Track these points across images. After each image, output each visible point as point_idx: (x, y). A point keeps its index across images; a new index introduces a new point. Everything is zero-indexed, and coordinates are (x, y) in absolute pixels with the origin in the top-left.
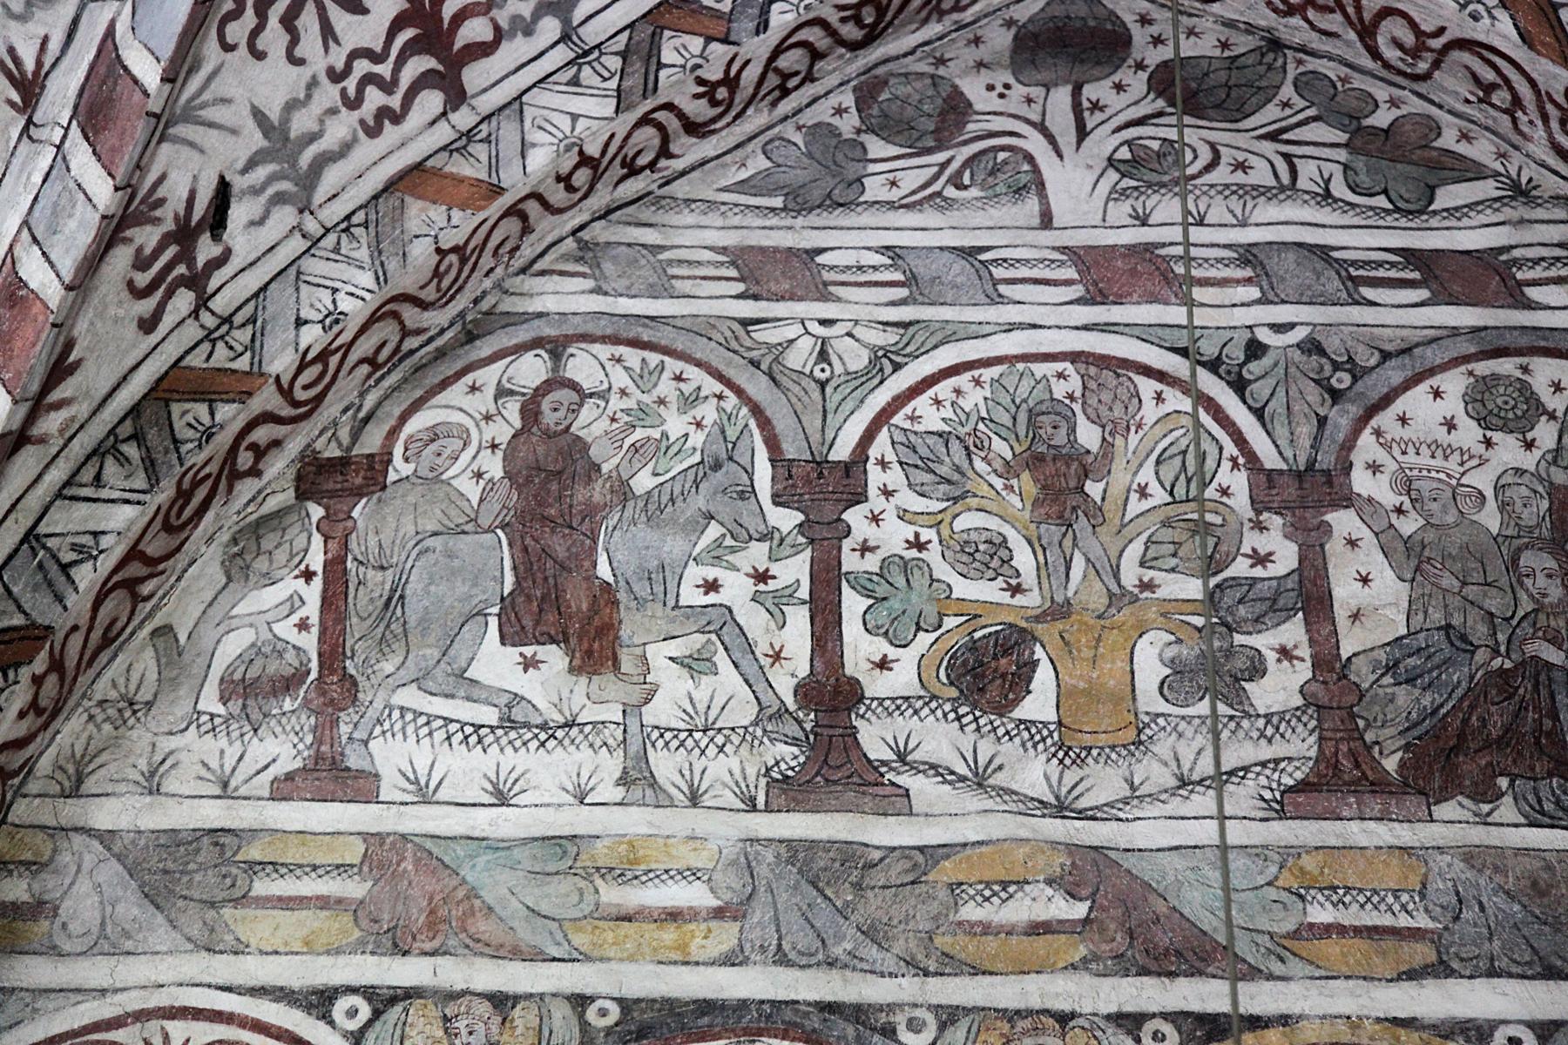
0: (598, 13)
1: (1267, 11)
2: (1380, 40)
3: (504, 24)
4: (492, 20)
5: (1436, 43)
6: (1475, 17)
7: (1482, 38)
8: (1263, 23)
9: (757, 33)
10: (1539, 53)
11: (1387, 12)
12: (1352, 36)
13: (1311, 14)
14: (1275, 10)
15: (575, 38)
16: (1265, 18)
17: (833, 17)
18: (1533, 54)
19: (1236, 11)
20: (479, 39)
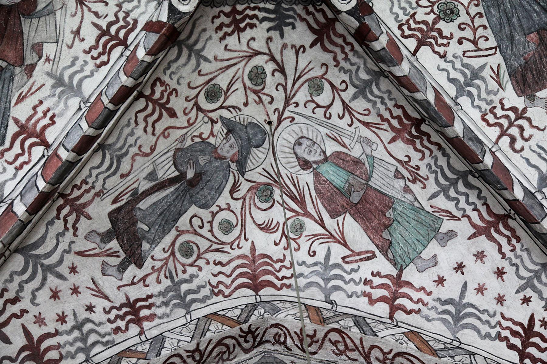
0: (99, 353)
1: (334, 355)
2: (372, 359)
3: (64, 354)
4: (59, 352)
5: (390, 356)
6: (401, 344)
7: (405, 351)
8: (332, 360)
9: (157, 356)
10: (424, 353)
11: (373, 347)
12: (362, 359)
13: (348, 353)
14: (336, 354)
15: (90, 361)
16: (333, 358)
17: (184, 355)
18: (422, 353)
19: (323, 356)
20: (54, 358)
